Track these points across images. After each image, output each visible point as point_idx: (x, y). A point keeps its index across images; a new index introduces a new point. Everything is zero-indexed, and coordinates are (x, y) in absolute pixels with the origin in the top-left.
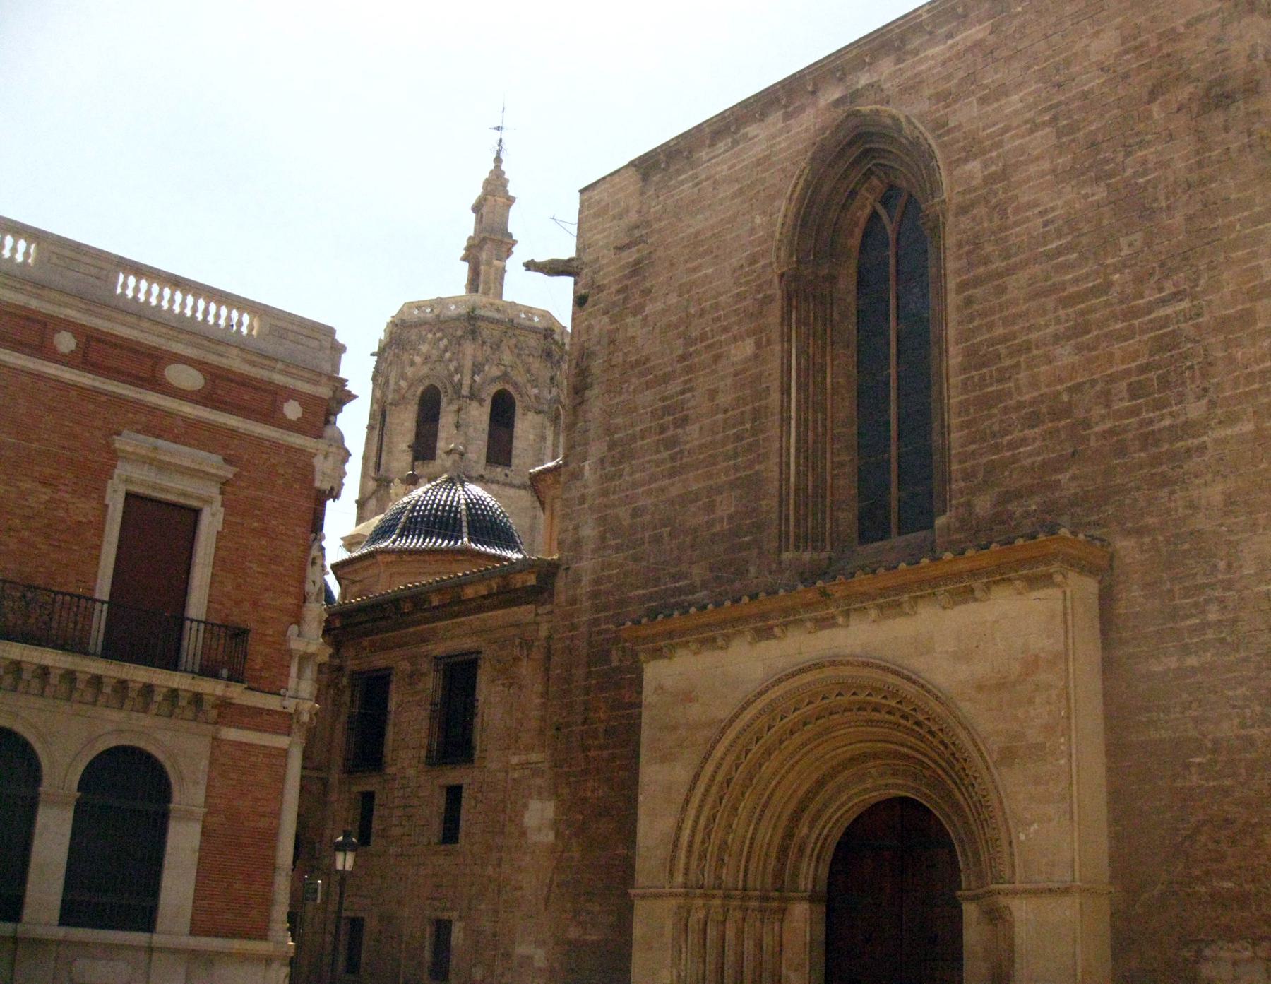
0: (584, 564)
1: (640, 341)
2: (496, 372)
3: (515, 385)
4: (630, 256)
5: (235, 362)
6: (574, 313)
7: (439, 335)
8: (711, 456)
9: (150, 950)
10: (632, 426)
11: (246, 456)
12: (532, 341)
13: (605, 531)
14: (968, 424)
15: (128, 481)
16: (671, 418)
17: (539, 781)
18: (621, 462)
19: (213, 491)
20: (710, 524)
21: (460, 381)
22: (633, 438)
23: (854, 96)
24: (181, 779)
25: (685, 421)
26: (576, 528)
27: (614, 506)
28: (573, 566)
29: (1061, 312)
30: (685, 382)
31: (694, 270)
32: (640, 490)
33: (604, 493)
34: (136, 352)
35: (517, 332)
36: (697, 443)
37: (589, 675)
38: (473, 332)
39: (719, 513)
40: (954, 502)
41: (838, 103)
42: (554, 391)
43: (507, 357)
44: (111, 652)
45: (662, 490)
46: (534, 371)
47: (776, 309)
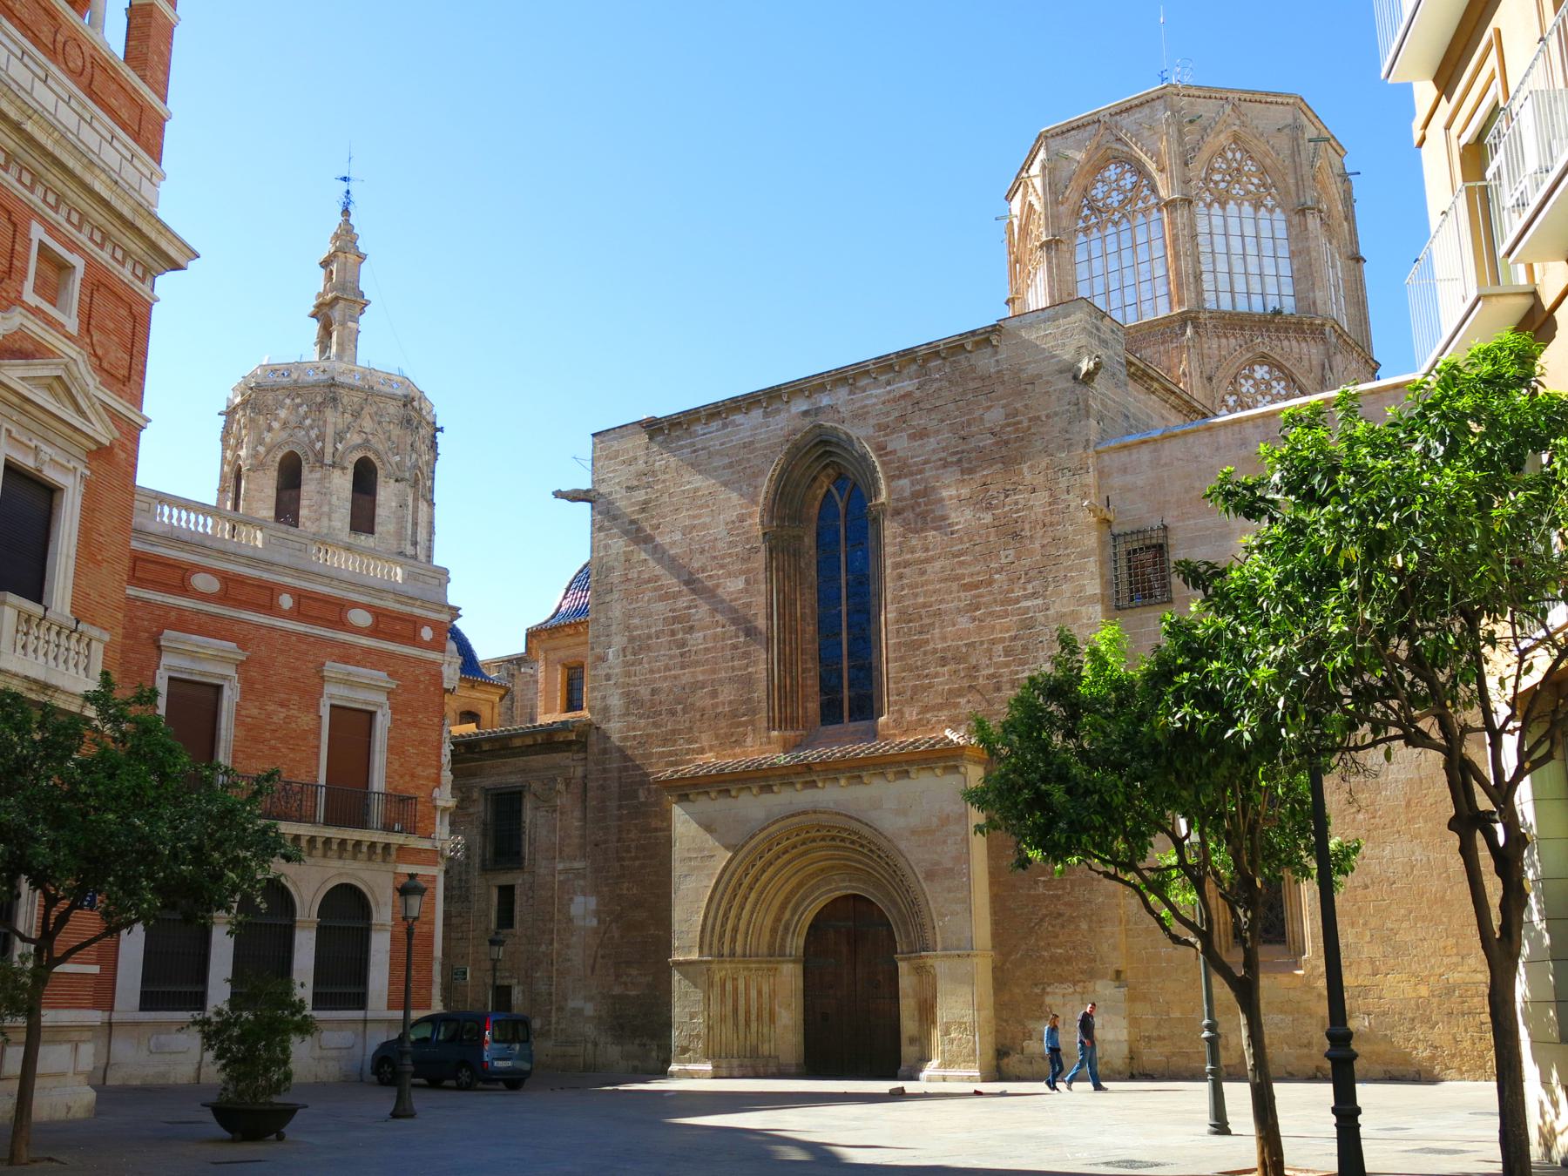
0: (611, 725)
2: (354, 438)
3: (376, 452)
5: (390, 604)
7: (298, 401)
9: (365, 1021)
12: (393, 408)
14: (901, 658)
15: (331, 697)
19: (382, 698)
20: (715, 706)
21: (322, 449)
22: (649, 637)
23: (818, 411)
24: (377, 904)
26: (604, 698)
29: (962, 594)
31: (694, 517)
34: (327, 602)
35: (377, 399)
37: (620, 807)
38: (334, 399)
39: (721, 698)
41: (806, 413)
42: (414, 456)
43: (368, 425)
44: (328, 822)
45: (675, 677)
46: (394, 438)
47: (761, 557)
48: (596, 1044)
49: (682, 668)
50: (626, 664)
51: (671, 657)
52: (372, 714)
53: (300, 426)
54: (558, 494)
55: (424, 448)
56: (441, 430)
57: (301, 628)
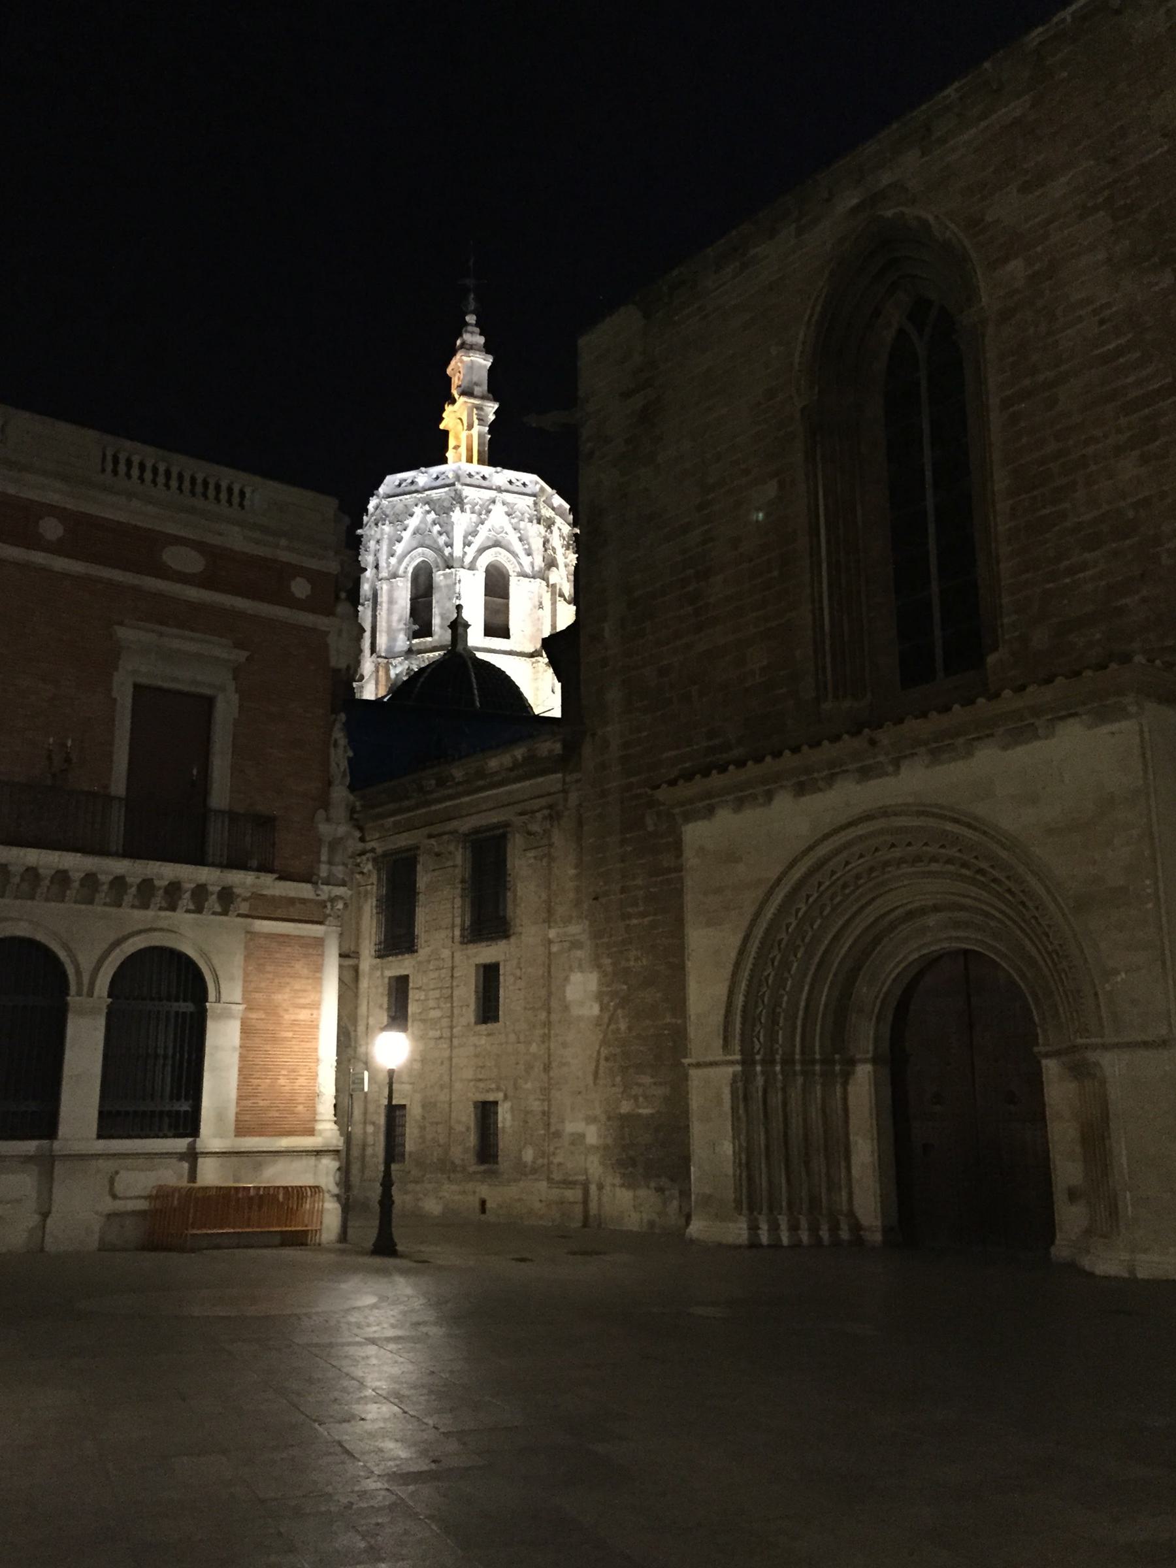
17: (579, 953)
29: (1123, 421)
40: (1007, 637)
41: (855, 210)
44: (130, 852)
48: (600, 1187)
52: (210, 701)
57: (77, 567)
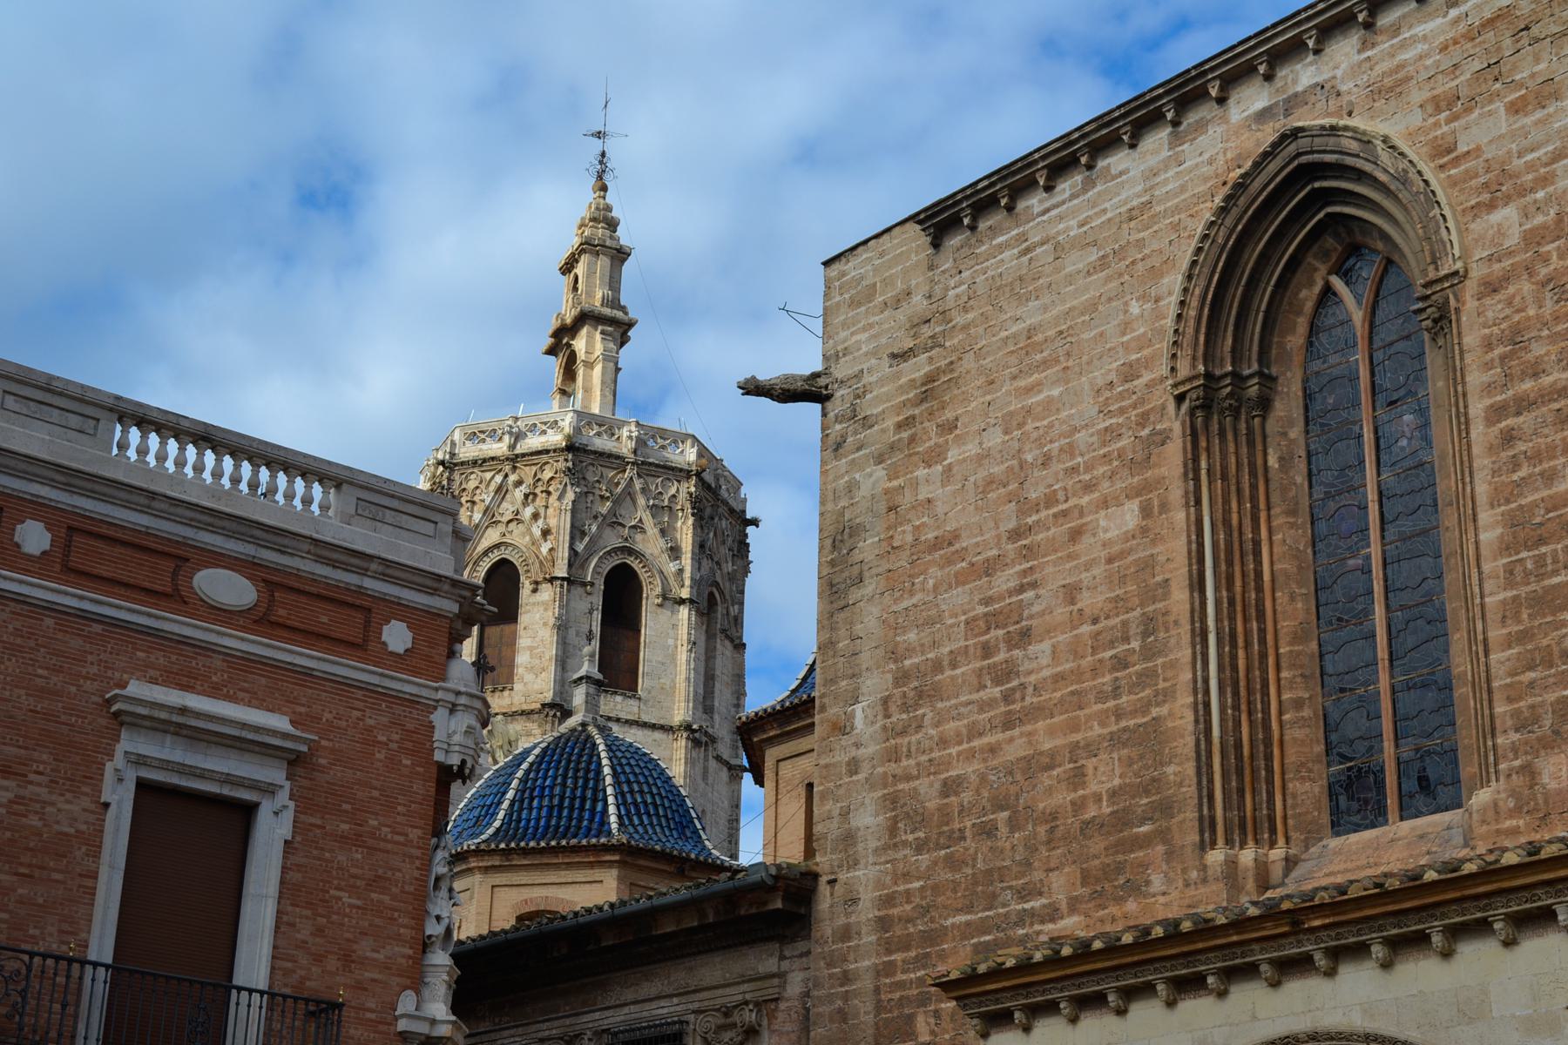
1: (940, 508)
4: (918, 368)
6: (823, 463)
8: (1072, 693)
10: (935, 644)
11: (327, 716)
13: (895, 820)
14: (1524, 636)
15: (139, 761)
16: (1001, 632)
18: (917, 706)
20: (1078, 806)
22: (937, 667)
23: (1293, 103)
25: (1025, 637)
26: (845, 814)
27: (908, 778)
28: (842, 876)
30: (1025, 573)
31: (1029, 390)
32: (954, 751)
33: (893, 755)
36: (1046, 673)
39: (1093, 787)
40: (1502, 767)
41: (1263, 115)
45: (993, 750)
47: (1174, 454)
49: (1008, 724)
50: (891, 732)
51: (983, 706)
53: (516, 519)
54: (753, 388)
55: (724, 551)
56: (755, 522)
